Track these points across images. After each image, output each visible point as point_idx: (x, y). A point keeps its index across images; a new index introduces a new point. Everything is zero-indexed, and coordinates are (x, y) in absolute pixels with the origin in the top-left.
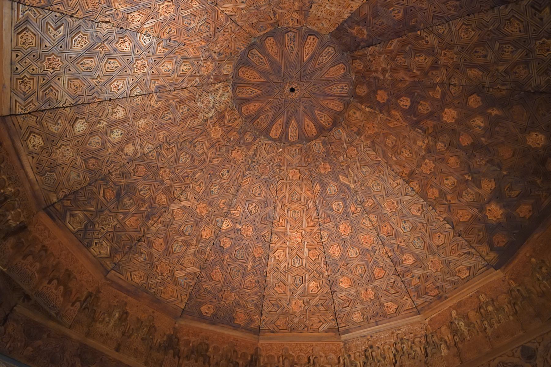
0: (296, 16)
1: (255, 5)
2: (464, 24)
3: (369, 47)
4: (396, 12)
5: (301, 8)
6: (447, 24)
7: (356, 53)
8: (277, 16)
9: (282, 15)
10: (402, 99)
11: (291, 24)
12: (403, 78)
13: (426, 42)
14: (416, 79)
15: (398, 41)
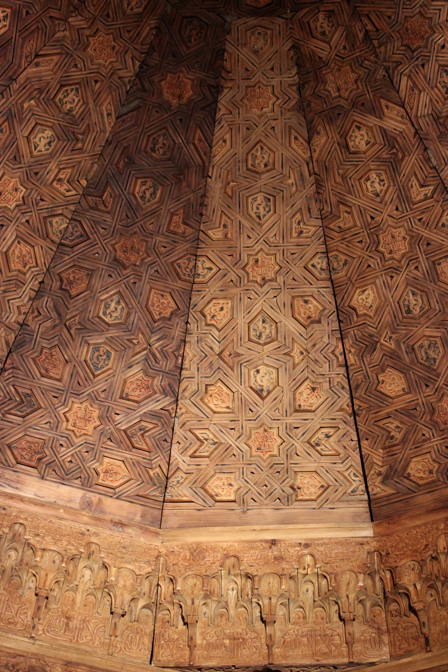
0: (322, 50)
1: (420, 62)
2: (37, 266)
3: (141, 67)
4: (148, 195)
5: (320, 80)
6: (57, 240)
7: (153, 22)
8: (361, 36)
9: (350, 36)
10: (7, 23)
11: (321, 16)
12: (37, 65)
13: (60, 180)
14: (15, 86)
15: (103, 131)
